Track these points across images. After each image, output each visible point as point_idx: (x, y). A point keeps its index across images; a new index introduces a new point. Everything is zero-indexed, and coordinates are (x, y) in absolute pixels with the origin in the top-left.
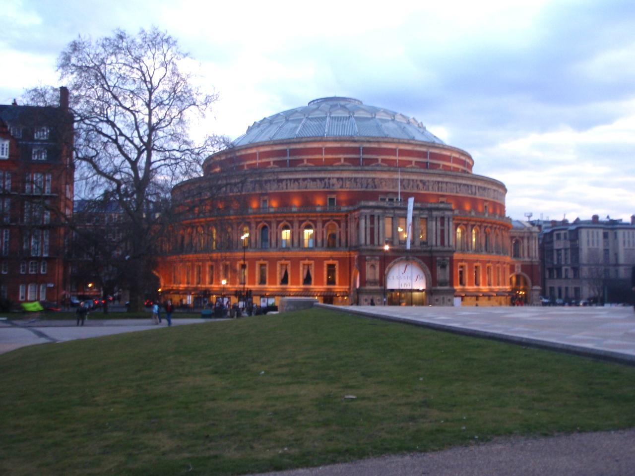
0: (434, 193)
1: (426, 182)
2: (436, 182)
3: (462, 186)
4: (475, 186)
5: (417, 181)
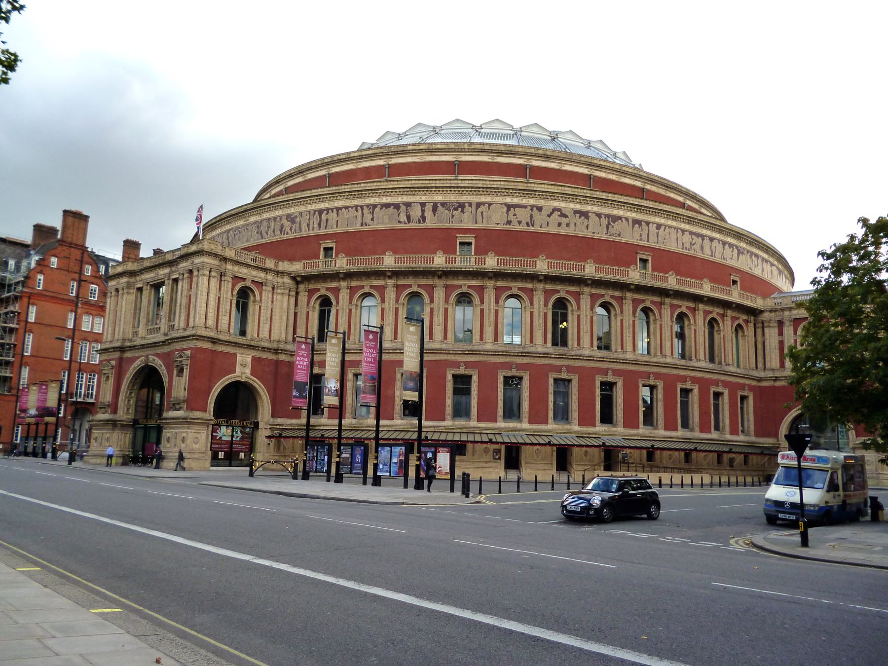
0: (311, 233)
1: (296, 217)
2: (315, 211)
3: (377, 210)
4: (423, 205)
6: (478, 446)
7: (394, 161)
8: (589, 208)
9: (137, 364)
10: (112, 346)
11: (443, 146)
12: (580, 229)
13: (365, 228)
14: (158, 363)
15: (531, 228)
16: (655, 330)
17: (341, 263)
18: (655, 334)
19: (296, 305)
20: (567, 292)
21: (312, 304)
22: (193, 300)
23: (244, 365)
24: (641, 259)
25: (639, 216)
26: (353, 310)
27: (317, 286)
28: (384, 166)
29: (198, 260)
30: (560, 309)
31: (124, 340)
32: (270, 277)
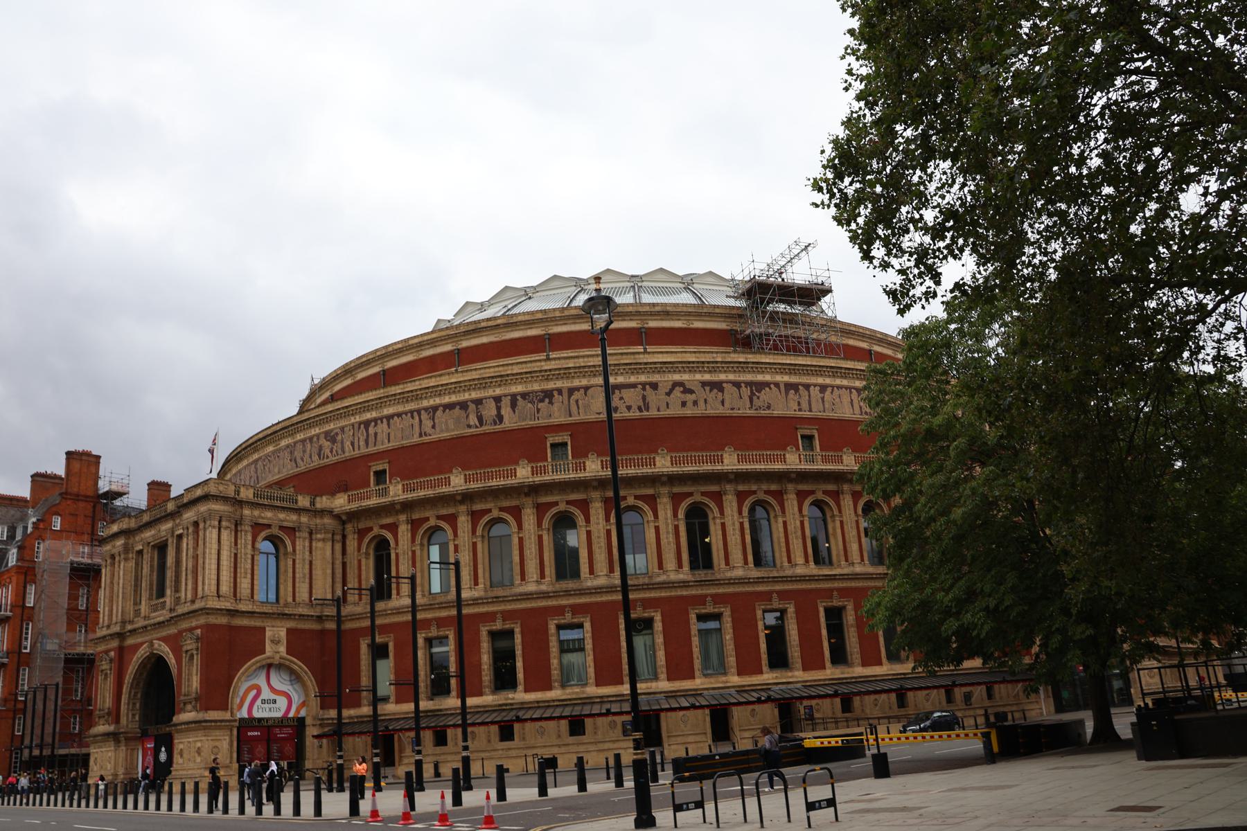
2: (360, 423)
3: (439, 413)
4: (497, 399)
5: (318, 436)
6: (600, 720)
7: (465, 344)
8: (722, 377)
9: (142, 652)
10: (109, 632)
11: (527, 318)
12: (713, 407)
13: (426, 439)
14: (165, 650)
15: (645, 413)
16: (834, 529)
17: (396, 491)
18: (836, 538)
19: (344, 552)
20: (703, 494)
21: (364, 550)
22: (200, 561)
23: (276, 642)
24: (803, 437)
25: (794, 379)
26: (418, 553)
27: (369, 524)
28: (452, 351)
29: (203, 508)
30: (697, 522)
31: (124, 622)
32: (304, 519)
